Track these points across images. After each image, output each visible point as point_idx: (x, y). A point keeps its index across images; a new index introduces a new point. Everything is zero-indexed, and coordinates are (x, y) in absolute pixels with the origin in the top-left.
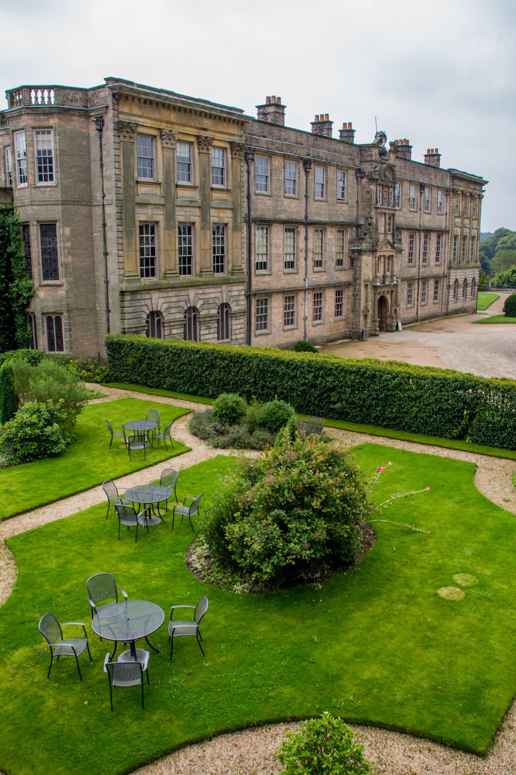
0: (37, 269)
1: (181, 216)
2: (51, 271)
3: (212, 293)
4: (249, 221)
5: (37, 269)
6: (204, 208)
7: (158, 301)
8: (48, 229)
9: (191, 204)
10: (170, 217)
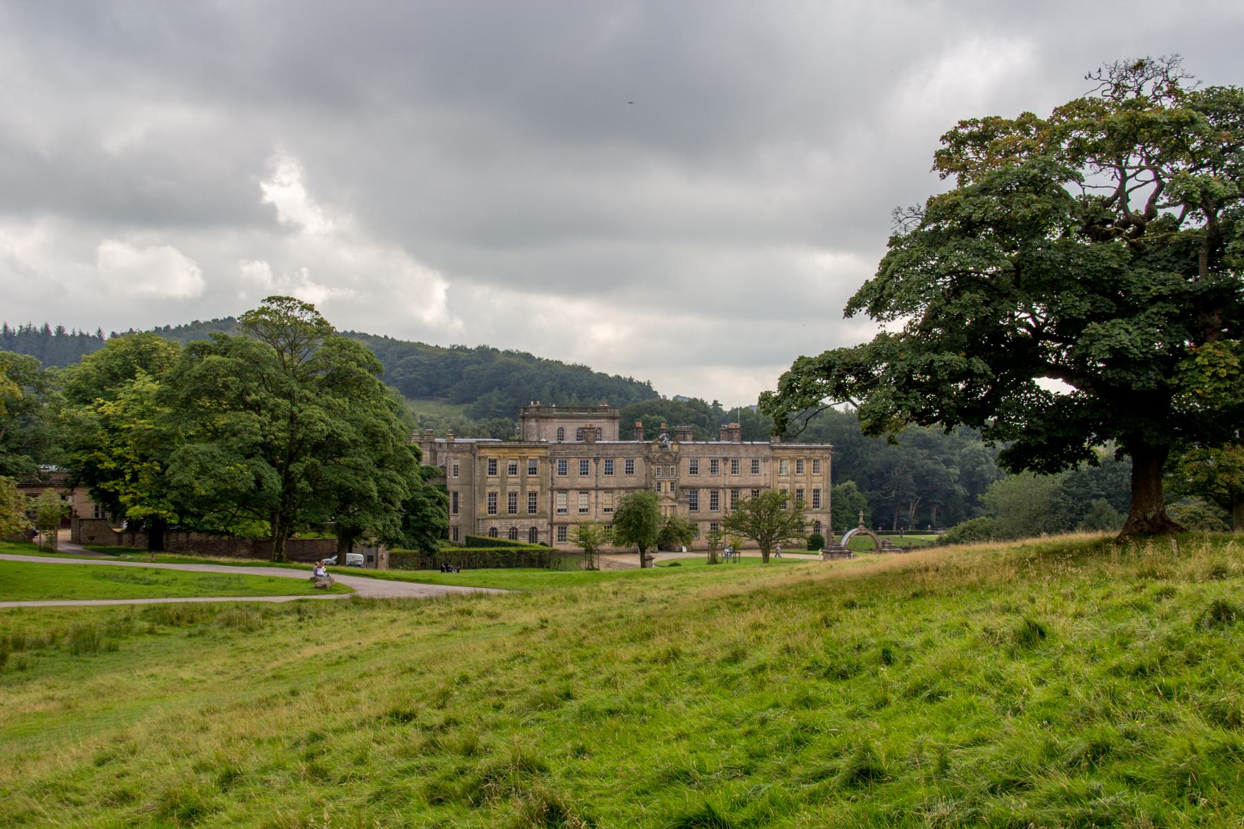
0: (451, 509)
1: (510, 489)
2: (456, 511)
3: (526, 522)
4: (552, 490)
5: (451, 509)
6: (523, 485)
7: (495, 524)
8: (456, 494)
9: (516, 484)
10: (503, 491)
